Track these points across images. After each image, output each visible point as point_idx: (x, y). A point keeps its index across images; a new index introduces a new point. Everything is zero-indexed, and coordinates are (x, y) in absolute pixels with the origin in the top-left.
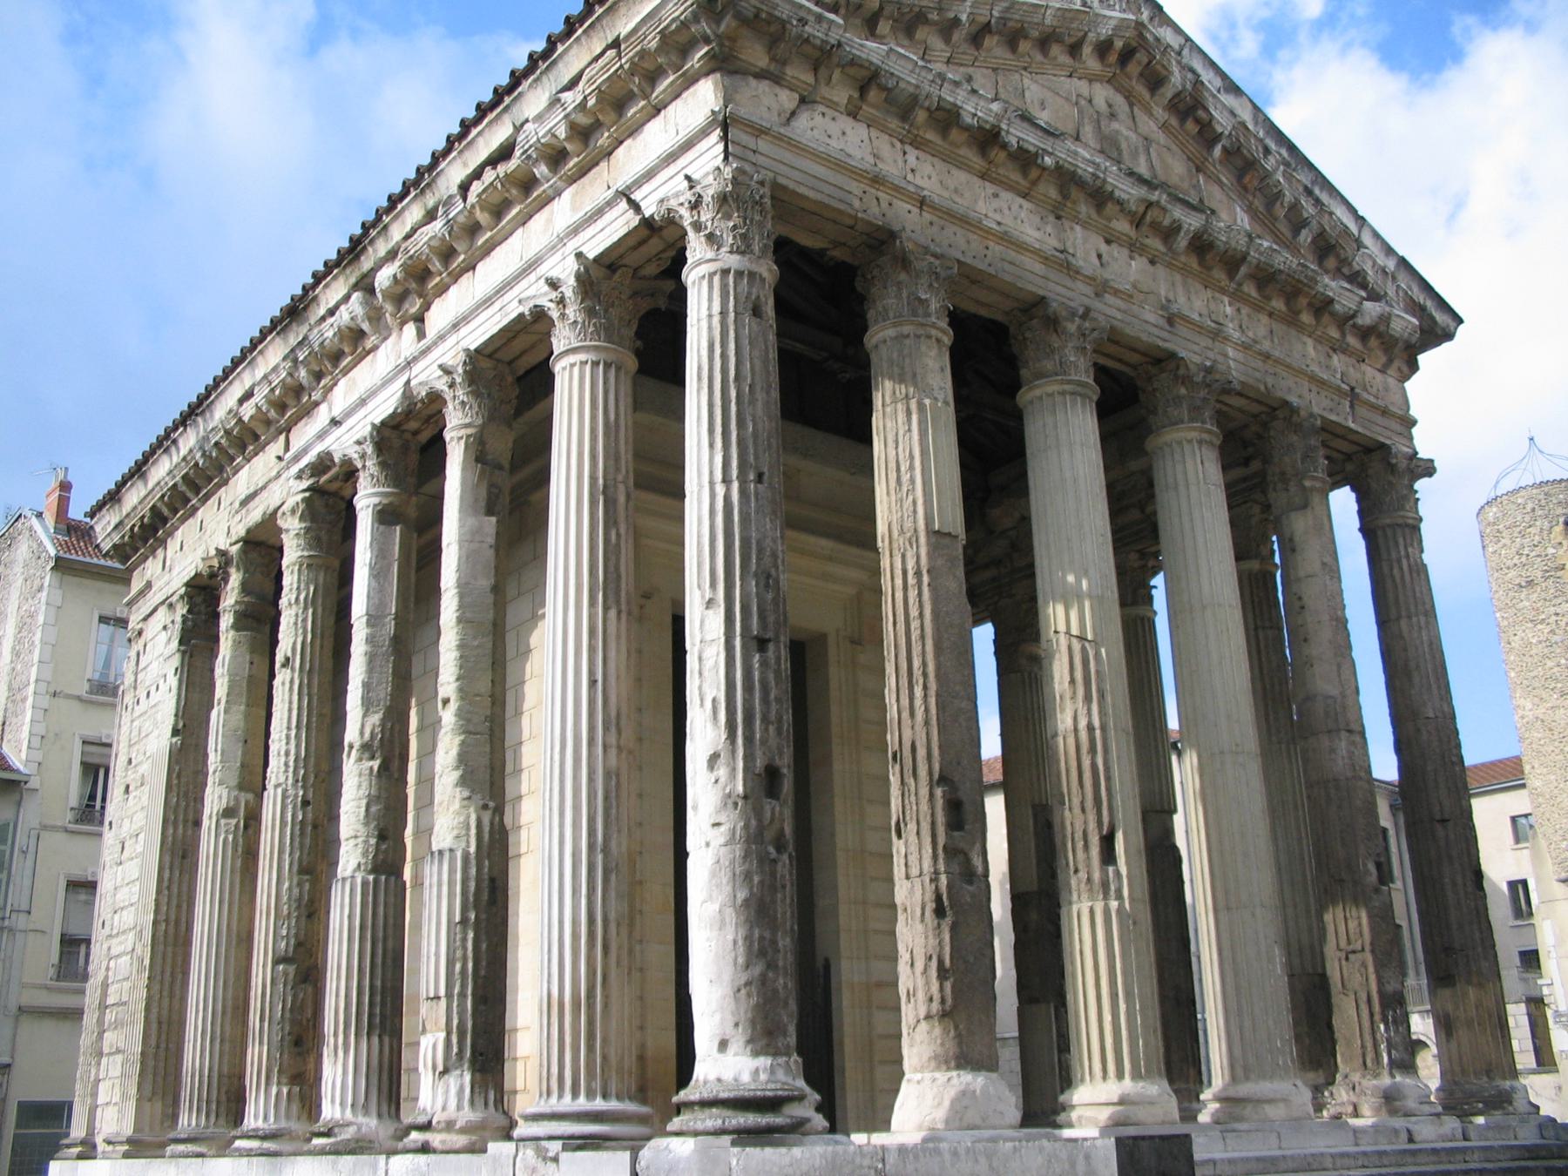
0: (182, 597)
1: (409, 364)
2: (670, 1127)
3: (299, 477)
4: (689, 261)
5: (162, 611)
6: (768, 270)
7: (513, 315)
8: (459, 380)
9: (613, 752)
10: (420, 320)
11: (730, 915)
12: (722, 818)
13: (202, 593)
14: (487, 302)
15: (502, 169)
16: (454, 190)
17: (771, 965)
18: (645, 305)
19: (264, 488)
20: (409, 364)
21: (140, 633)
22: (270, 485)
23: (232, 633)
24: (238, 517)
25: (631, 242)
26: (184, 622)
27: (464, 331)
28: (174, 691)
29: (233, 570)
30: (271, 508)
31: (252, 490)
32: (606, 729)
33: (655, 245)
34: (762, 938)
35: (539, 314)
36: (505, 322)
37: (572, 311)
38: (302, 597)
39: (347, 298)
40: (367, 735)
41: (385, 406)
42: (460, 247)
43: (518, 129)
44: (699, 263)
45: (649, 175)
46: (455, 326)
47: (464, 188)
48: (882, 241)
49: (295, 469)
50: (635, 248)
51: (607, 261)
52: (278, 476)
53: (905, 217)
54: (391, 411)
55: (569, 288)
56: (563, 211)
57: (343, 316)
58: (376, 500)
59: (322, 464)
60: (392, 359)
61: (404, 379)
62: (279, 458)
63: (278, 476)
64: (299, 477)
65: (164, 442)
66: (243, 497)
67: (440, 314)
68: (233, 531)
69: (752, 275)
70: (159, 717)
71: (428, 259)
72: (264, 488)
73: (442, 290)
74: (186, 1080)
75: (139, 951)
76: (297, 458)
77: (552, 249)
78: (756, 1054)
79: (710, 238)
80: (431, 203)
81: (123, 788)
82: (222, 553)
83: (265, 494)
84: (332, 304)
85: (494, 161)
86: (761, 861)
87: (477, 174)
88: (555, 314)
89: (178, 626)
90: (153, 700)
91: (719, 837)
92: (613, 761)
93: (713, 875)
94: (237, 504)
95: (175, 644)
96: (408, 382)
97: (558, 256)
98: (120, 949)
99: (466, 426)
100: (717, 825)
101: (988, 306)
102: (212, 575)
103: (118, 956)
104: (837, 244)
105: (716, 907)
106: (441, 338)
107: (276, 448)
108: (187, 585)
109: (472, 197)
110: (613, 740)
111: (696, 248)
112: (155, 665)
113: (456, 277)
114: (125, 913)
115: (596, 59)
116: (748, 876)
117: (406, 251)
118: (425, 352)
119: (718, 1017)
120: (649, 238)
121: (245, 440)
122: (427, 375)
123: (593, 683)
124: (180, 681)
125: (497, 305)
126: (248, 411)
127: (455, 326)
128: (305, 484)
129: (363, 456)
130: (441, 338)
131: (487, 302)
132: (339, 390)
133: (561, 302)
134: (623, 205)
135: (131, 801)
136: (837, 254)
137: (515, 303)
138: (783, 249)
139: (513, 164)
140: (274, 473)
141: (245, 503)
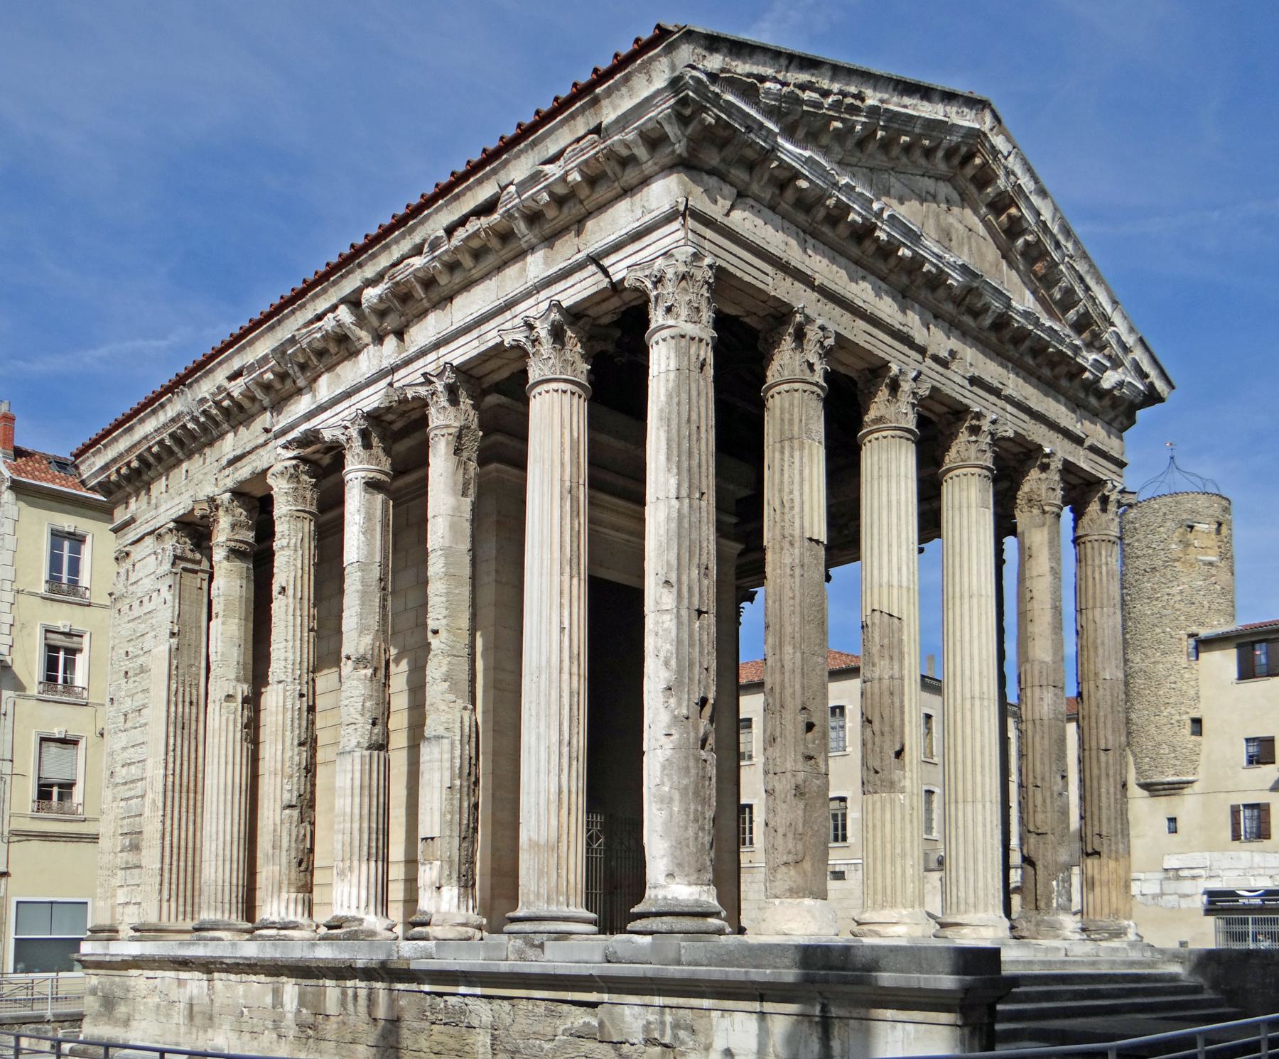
0: (171, 530)
1: (394, 370)
2: (629, 927)
4: (653, 326)
5: (149, 541)
6: (709, 334)
7: (491, 344)
8: (440, 388)
9: (575, 678)
10: (400, 334)
11: (677, 796)
12: (673, 732)
13: (195, 530)
14: (466, 330)
17: (702, 829)
18: (599, 347)
19: (249, 452)
20: (394, 370)
22: (264, 450)
24: (226, 472)
25: (597, 299)
26: (174, 550)
27: (442, 351)
28: (169, 604)
29: (221, 512)
30: (259, 470)
31: (238, 452)
32: (571, 662)
33: (615, 302)
34: (696, 810)
35: (517, 347)
36: (483, 348)
37: (546, 347)
38: (293, 541)
41: (372, 399)
44: (662, 328)
46: (437, 346)
48: (781, 316)
50: (598, 303)
51: (574, 311)
52: (265, 444)
53: (800, 298)
54: (376, 405)
55: (542, 330)
59: (311, 438)
60: (375, 362)
62: (267, 431)
63: (265, 444)
64: (285, 447)
65: (151, 404)
66: (231, 456)
67: (421, 334)
68: (221, 483)
69: (701, 340)
70: (154, 621)
72: (249, 452)
73: (423, 314)
74: (205, 888)
75: (150, 796)
76: (284, 432)
77: (527, 295)
78: (690, 884)
79: (669, 310)
81: (122, 673)
82: (211, 500)
83: (252, 457)
86: (697, 759)
88: (530, 350)
89: (170, 553)
90: (148, 607)
91: (668, 744)
92: (575, 685)
93: (664, 768)
94: (224, 462)
95: (167, 566)
96: (391, 385)
97: (531, 301)
98: (132, 793)
101: (851, 366)
102: (203, 517)
103: (127, 799)
104: (749, 314)
105: (667, 789)
106: (423, 353)
107: (266, 419)
108: (174, 521)
110: (575, 670)
111: (657, 317)
112: (145, 581)
114: (133, 767)
116: (687, 769)
117: (392, 277)
118: (407, 362)
119: (665, 860)
120: (611, 297)
121: (236, 414)
122: (409, 376)
123: (562, 629)
124: (174, 595)
125: (475, 333)
127: (437, 346)
128: (291, 454)
130: (423, 353)
131: (466, 330)
132: (324, 380)
133: (535, 341)
135: (131, 685)
136: (747, 320)
137: (495, 333)
138: (721, 322)
140: (261, 441)
141: (231, 463)
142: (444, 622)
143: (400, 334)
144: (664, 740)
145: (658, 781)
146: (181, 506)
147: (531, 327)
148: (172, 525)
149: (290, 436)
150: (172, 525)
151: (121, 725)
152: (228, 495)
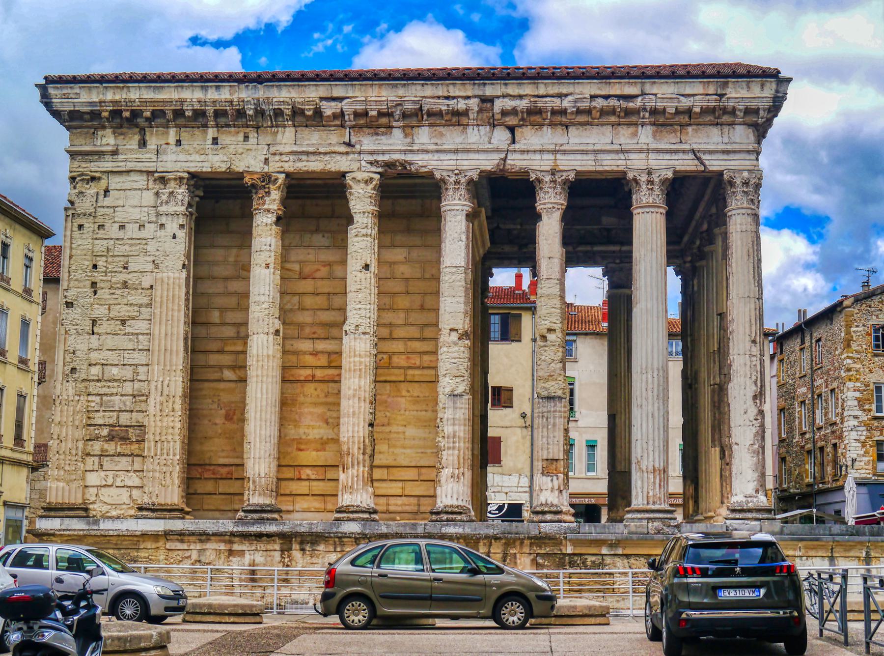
0: (181, 178)
3: (371, 163)
15: (624, 104)
16: (588, 96)
21: (99, 178)
23: (274, 227)
36: (601, 168)
39: (468, 97)
40: (466, 328)
42: (569, 117)
43: (643, 94)
45: (711, 152)
47: (593, 97)
49: (371, 158)
54: (489, 168)
56: (646, 136)
57: (461, 105)
58: (467, 208)
61: (503, 156)
64: (371, 163)
71: (547, 112)
72: (320, 153)
80: (565, 91)
84: (452, 94)
85: (619, 97)
87: (606, 97)
93: (755, 436)
99: (562, 205)
100: (756, 419)
105: (757, 446)
108: (189, 173)
109: (594, 104)
113: (552, 124)
115: (707, 95)
126: (329, 109)
129: (457, 182)
134: (691, 156)
139: (631, 105)
142: (560, 325)
143: (512, 129)
144: (755, 422)
145: (752, 442)
146: (205, 164)
147: (649, 173)
148: (186, 175)
149: (380, 158)
150: (186, 175)
151: (88, 328)
152: (283, 176)
